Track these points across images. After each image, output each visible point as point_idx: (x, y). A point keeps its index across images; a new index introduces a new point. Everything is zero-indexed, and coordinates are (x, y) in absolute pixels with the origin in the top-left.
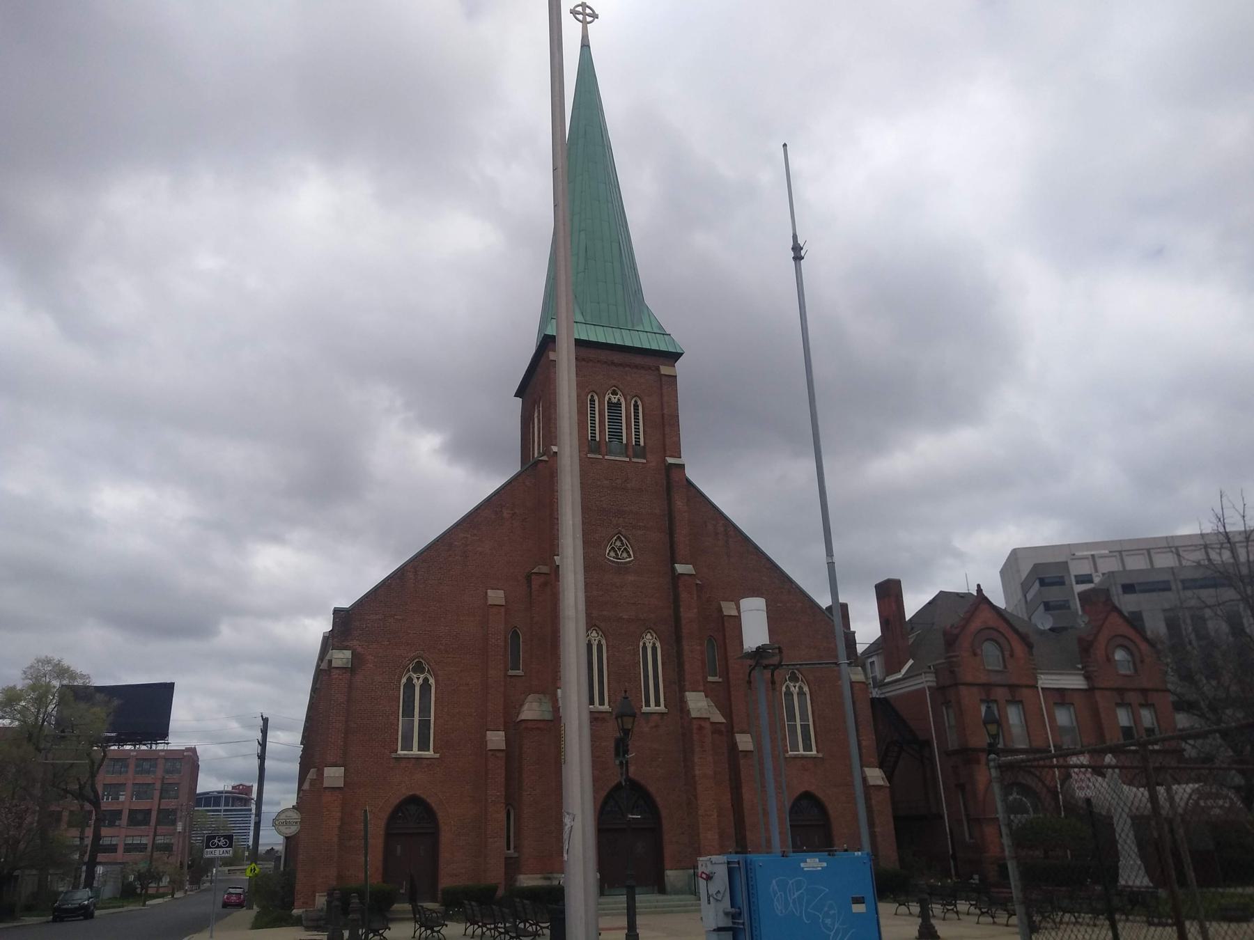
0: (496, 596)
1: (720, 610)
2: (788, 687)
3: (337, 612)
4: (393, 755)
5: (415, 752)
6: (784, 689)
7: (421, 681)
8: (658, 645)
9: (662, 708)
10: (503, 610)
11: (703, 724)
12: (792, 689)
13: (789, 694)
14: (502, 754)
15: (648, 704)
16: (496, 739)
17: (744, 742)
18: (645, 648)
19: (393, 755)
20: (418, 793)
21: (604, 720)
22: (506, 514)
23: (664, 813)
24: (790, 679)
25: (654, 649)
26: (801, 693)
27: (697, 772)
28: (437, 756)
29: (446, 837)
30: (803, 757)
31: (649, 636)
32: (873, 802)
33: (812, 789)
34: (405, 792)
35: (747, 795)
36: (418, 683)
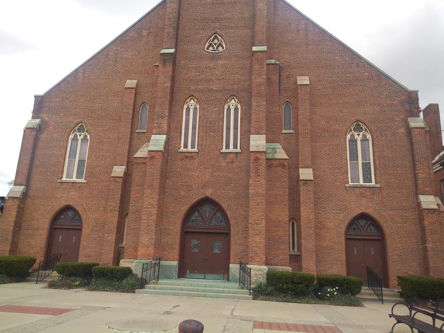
0: (131, 83)
2: (352, 136)
3: (36, 97)
5: (74, 179)
6: (348, 136)
7: (82, 137)
8: (239, 106)
9: (239, 150)
10: (134, 91)
11: (259, 156)
12: (356, 137)
13: (353, 141)
14: (121, 180)
15: (228, 147)
16: (119, 171)
17: (306, 174)
18: (229, 109)
19: (59, 181)
20: (71, 204)
22: (144, 33)
23: (232, 222)
25: (236, 109)
26: (364, 140)
28: (85, 181)
29: (85, 231)
30: (362, 187)
31: (233, 101)
32: (426, 223)
33: (370, 211)
34: (64, 203)
35: (306, 212)
36: (80, 138)
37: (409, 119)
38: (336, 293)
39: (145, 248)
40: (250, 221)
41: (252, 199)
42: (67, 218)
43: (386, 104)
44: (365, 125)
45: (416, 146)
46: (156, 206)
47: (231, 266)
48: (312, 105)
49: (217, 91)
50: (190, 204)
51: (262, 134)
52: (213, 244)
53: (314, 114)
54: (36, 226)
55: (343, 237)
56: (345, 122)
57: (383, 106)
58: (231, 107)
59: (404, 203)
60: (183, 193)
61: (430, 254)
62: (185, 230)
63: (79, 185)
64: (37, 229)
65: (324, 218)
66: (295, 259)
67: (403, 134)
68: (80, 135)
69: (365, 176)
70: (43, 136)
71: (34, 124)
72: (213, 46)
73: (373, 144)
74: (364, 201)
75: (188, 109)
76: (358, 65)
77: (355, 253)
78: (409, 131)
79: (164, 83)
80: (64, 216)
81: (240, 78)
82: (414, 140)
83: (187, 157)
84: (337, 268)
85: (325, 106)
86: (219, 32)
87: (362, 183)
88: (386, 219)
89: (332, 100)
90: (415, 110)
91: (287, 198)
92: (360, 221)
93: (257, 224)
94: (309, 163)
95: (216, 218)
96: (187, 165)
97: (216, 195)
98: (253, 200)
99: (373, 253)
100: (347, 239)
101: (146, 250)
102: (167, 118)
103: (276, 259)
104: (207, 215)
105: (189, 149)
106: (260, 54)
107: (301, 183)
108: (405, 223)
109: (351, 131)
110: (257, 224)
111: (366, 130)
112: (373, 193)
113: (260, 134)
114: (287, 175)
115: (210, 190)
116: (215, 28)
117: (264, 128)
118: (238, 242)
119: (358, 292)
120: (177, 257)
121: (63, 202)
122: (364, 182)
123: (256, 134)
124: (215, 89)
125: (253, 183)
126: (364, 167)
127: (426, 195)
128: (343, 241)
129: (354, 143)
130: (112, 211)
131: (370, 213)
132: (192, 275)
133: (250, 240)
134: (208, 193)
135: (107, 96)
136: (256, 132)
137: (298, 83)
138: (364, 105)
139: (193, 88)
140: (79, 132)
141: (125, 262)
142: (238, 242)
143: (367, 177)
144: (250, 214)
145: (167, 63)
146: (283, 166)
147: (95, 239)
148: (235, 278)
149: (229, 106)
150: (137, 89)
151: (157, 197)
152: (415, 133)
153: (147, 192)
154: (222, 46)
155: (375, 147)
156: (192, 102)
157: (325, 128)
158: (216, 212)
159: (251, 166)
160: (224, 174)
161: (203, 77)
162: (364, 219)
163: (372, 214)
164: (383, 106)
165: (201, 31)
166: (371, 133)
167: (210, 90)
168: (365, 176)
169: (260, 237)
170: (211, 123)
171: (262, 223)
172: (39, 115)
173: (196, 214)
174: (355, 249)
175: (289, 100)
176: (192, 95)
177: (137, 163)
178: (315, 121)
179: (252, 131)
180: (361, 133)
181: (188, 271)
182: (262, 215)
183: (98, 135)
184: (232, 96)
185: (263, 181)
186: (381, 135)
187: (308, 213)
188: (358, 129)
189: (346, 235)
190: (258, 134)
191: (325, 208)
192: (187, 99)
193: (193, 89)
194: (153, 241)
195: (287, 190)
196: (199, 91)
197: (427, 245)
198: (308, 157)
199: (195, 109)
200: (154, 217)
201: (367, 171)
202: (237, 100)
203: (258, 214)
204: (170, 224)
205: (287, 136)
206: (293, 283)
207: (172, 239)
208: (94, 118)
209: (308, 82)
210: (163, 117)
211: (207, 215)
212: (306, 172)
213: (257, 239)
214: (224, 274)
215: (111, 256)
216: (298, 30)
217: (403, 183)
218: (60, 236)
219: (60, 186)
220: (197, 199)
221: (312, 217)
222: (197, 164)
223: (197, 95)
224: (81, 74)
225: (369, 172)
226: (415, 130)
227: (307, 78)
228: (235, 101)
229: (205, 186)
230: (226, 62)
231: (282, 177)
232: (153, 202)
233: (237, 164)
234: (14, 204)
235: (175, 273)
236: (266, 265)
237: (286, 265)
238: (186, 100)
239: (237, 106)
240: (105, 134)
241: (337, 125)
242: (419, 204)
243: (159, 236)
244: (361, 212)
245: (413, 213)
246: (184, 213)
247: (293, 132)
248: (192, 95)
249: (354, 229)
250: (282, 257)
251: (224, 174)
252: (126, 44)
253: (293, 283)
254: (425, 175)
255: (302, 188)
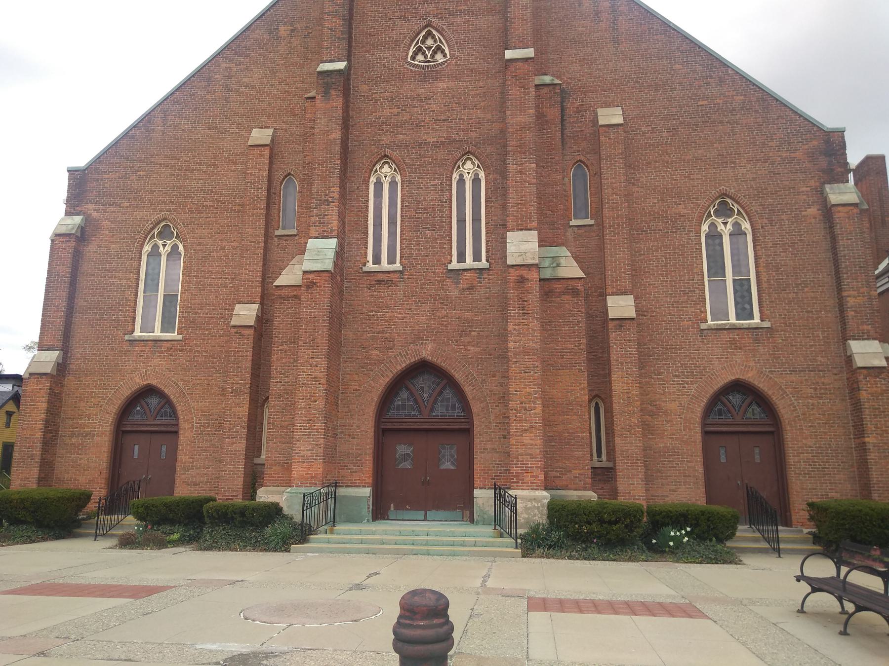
0: (261, 135)
1: (595, 120)
2: (713, 226)
3: (71, 171)
4: (127, 337)
5: (158, 333)
6: (705, 228)
7: (168, 248)
8: (482, 175)
9: (484, 263)
10: (267, 151)
12: (721, 227)
13: (714, 237)
14: (251, 332)
15: (461, 258)
16: (246, 313)
17: (621, 306)
18: (461, 181)
19: (127, 337)
20: (154, 382)
21: (390, 283)
22: (283, 31)
23: (476, 408)
24: (718, 213)
25: (476, 181)
26: (738, 233)
27: (511, 345)
28: (180, 337)
29: (186, 435)
30: (733, 328)
31: (469, 165)
32: (864, 395)
33: (750, 376)
34: (139, 382)
35: (622, 383)
37: (827, 188)
38: (686, 539)
39: (305, 465)
40: (512, 404)
41: (514, 360)
42: (147, 410)
43: (779, 159)
44: (738, 203)
45: (842, 242)
46: (323, 381)
47: (477, 493)
48: (630, 166)
49: (435, 145)
50: (391, 375)
51: (531, 229)
52: (440, 452)
53: (634, 184)
54: (87, 430)
55: (698, 430)
56: (697, 199)
57: (773, 164)
58: (466, 176)
59: (819, 358)
60: (375, 354)
61: (872, 456)
62: (384, 426)
63: (169, 345)
64: (91, 435)
65: (660, 394)
66: (604, 476)
67: (815, 218)
68: (164, 246)
69: (739, 306)
70: (91, 249)
71: (70, 226)
72: (424, 53)
73: (754, 241)
74: (739, 357)
75: (379, 185)
76: (721, 81)
77: (723, 459)
78: (828, 211)
79: (328, 133)
80: (142, 407)
81: (482, 116)
82: (837, 231)
83: (380, 282)
84: (686, 491)
85: (655, 168)
86: (435, 22)
87: (733, 320)
88: (782, 390)
89: (669, 155)
90: (839, 169)
91: (584, 356)
92: (731, 397)
93: (525, 409)
94: (627, 284)
95: (442, 401)
96: (382, 298)
97: (442, 356)
98: (516, 363)
99: (757, 459)
100: (706, 433)
101: (308, 468)
102: (336, 204)
103: (564, 477)
104: (425, 395)
105: (385, 265)
106: (520, 64)
107: (611, 325)
108: (821, 398)
109: (709, 215)
110: (525, 409)
111: (739, 213)
112: (757, 340)
113: (527, 229)
114: (583, 310)
115: (430, 346)
116: (427, 14)
117: (534, 218)
118: (489, 446)
119: (731, 537)
120: (370, 481)
121: (138, 381)
122: (738, 318)
123: (518, 230)
124: (432, 140)
125: (515, 330)
126: (738, 288)
127: (863, 339)
128: (699, 437)
129: (717, 241)
130: (236, 394)
131: (751, 380)
132: (401, 514)
133: (513, 442)
134: (427, 351)
135: (214, 164)
136: (518, 225)
137: (601, 122)
138: (734, 163)
139: (386, 139)
140: (161, 239)
141: (266, 492)
142: (489, 446)
143: (744, 309)
144: (512, 390)
145: (333, 92)
146: (575, 292)
147: (205, 451)
148: (486, 516)
149: (461, 176)
150: (273, 147)
151: (324, 364)
152: (839, 216)
153: (304, 353)
154: (443, 51)
155: (758, 248)
156: (386, 169)
157: (658, 213)
158: (444, 388)
159: (510, 296)
160: (456, 313)
161: (406, 117)
162: (739, 392)
163: (756, 383)
164: (773, 164)
165: (398, 23)
166: (749, 220)
167: (422, 145)
168: (739, 306)
169: (532, 435)
170: (426, 210)
171: (535, 408)
172: (80, 208)
173: (404, 394)
174: (722, 451)
175: (582, 158)
176: (386, 156)
177: (281, 297)
178: (637, 198)
179: (510, 224)
180: (730, 220)
181: (392, 505)
182: (536, 392)
183: (200, 244)
184: (467, 154)
185: (535, 325)
186: (771, 221)
187: (628, 384)
188: (724, 211)
189: (704, 425)
190: (521, 230)
191: (660, 374)
192: (376, 163)
193: (388, 142)
194: (321, 450)
195: (583, 341)
196: (399, 147)
197: (867, 440)
198: (625, 273)
199: (393, 183)
200: (321, 403)
201: (743, 297)
202: (477, 162)
203: (528, 390)
204: (352, 415)
205: (580, 231)
206: (602, 521)
207: (358, 444)
208: (190, 210)
209: (620, 120)
210: (329, 203)
211: (425, 395)
212: (622, 303)
213: (527, 438)
214: (462, 509)
215: (239, 482)
216: (597, 13)
217: (817, 319)
218: (137, 447)
219: (130, 349)
220: (404, 365)
221: (635, 392)
222: (400, 294)
223: (395, 154)
224: (158, 121)
225: (747, 299)
226: (840, 209)
227: (619, 111)
228: (473, 163)
229: (419, 338)
230: (451, 84)
231: (573, 315)
232: (318, 374)
233: (482, 291)
234: (41, 386)
235: (366, 510)
236: (546, 489)
237: (585, 489)
238: (374, 166)
239: (477, 175)
240: (214, 241)
241: (682, 206)
242: (849, 359)
243: (331, 439)
244: (733, 378)
245: (837, 377)
246: (379, 393)
247: (592, 222)
248: (386, 156)
249: (720, 412)
250: (576, 472)
251: (456, 313)
252: (248, 55)
253: (602, 521)
254: (860, 300)
255: (613, 335)
